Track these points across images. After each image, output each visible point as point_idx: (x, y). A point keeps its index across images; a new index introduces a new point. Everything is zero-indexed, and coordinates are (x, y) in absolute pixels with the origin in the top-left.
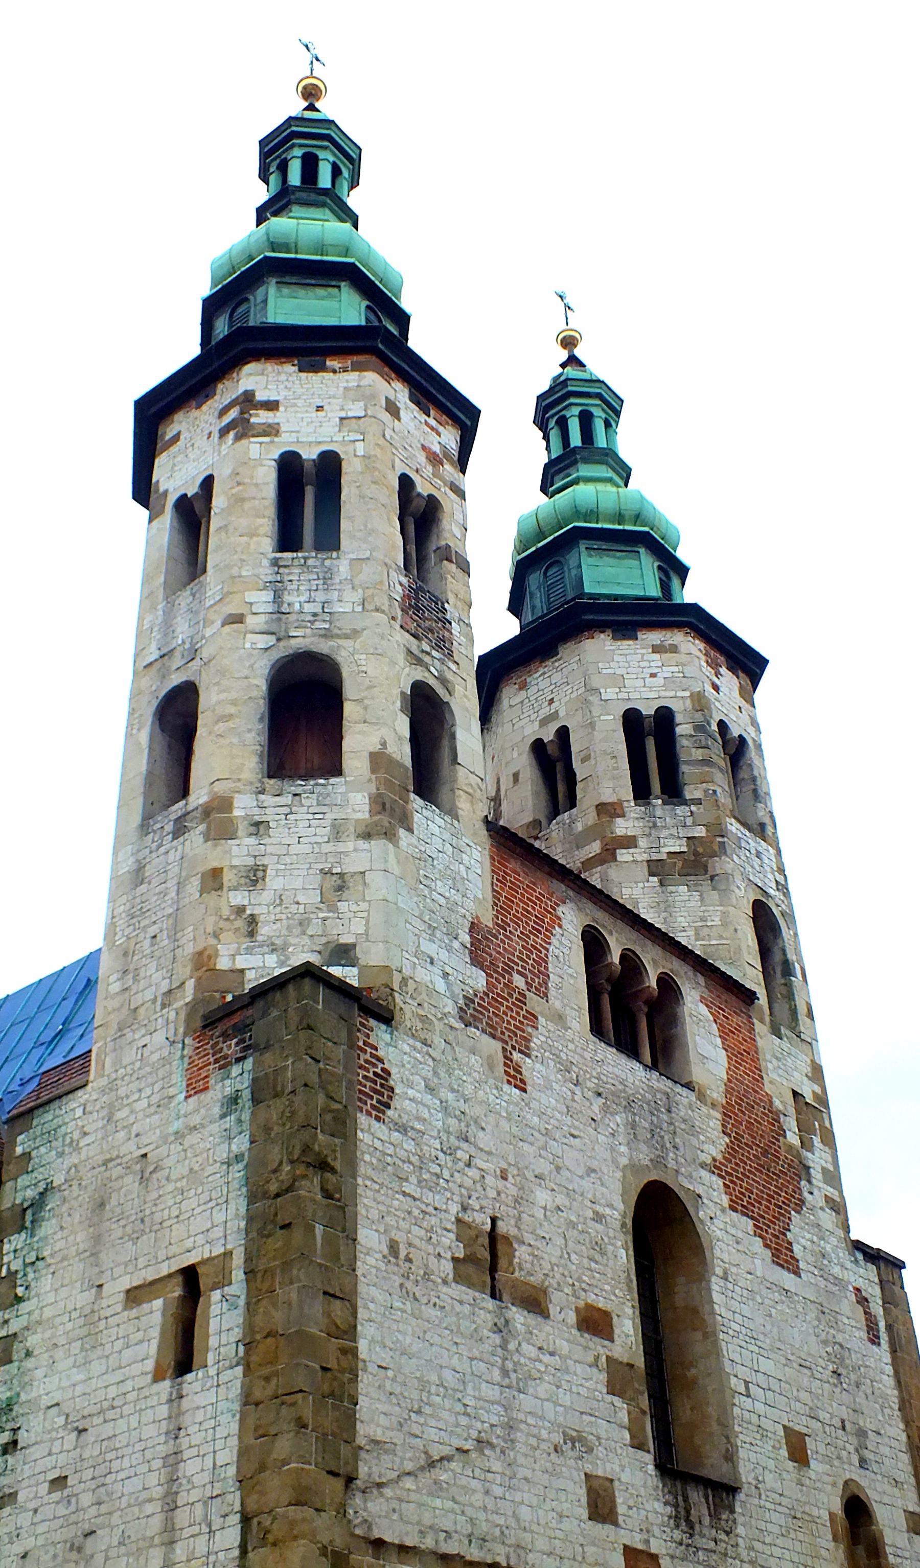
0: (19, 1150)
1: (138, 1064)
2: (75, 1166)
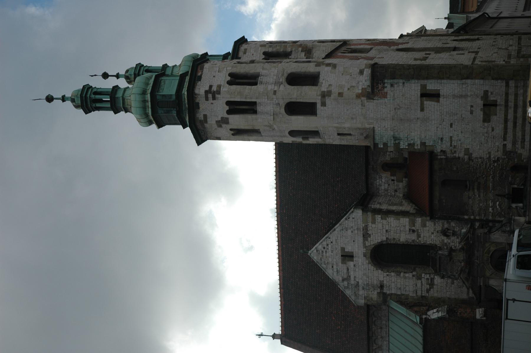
0: (382, 146)
1: (375, 113)
2: (391, 128)
